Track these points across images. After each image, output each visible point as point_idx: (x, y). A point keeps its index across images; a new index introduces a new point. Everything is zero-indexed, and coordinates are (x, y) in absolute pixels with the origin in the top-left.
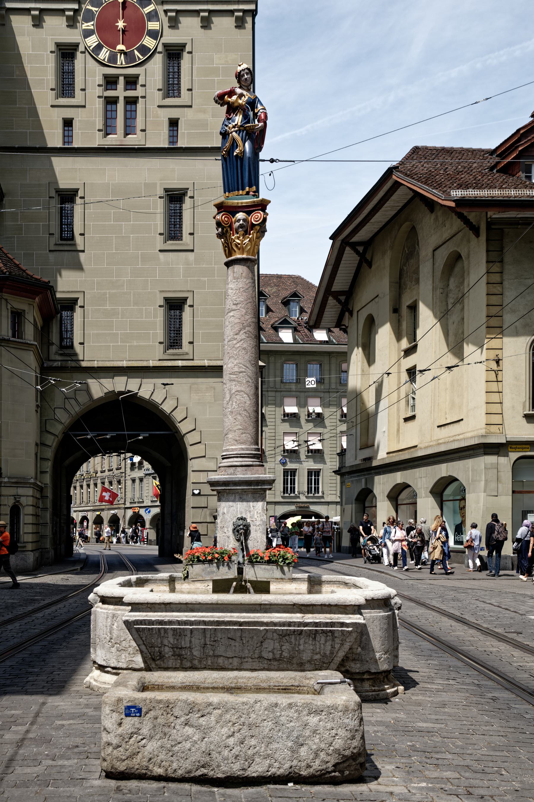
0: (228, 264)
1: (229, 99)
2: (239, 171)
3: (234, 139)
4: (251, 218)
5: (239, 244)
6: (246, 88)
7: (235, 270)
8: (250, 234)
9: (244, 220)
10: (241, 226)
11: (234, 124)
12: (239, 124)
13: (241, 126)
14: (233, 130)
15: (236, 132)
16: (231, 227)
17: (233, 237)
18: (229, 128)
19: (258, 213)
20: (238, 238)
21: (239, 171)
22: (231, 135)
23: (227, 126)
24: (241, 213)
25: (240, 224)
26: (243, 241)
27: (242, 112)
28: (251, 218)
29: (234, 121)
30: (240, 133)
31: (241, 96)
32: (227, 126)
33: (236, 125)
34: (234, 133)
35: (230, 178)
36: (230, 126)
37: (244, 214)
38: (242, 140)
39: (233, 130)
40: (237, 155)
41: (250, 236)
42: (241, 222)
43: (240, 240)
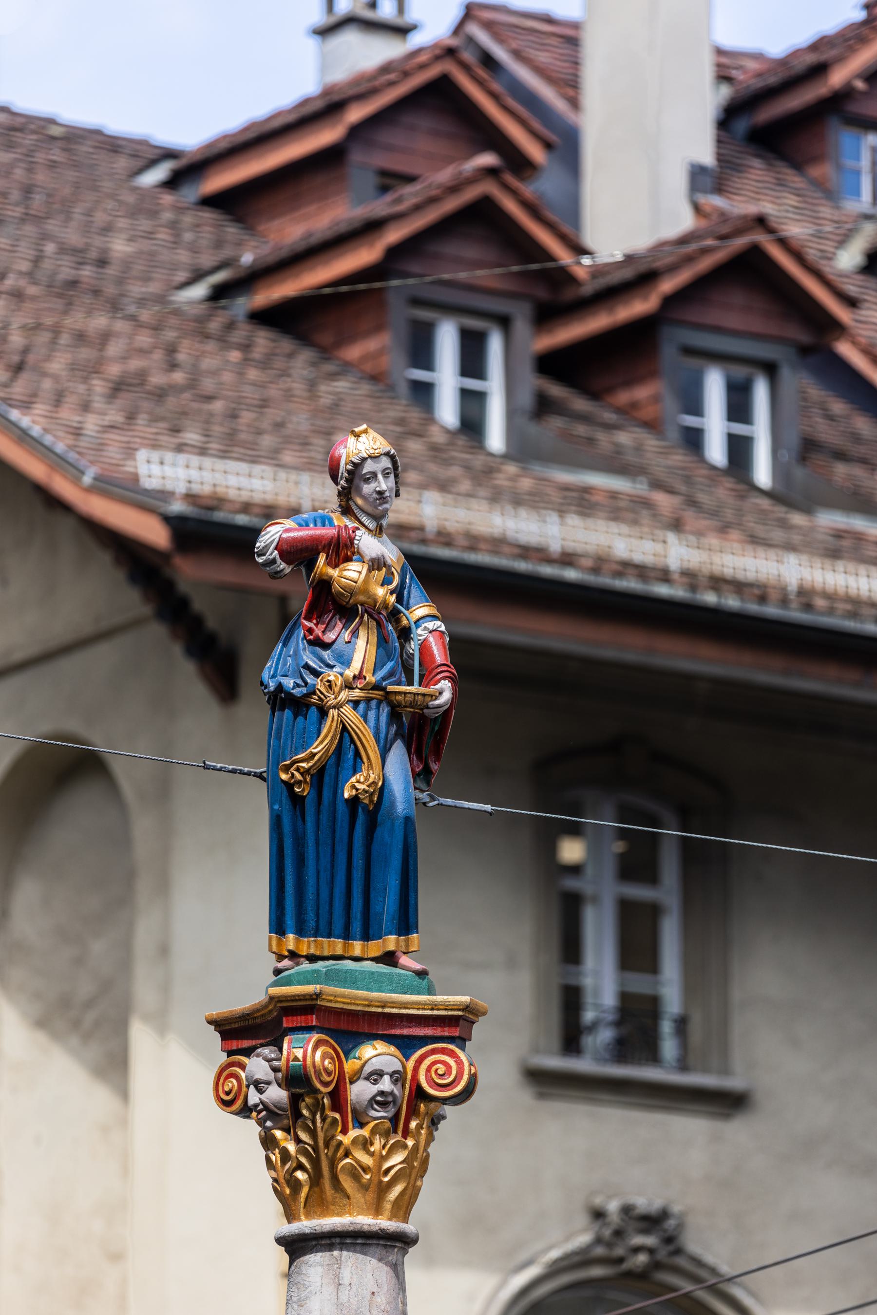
0: (296, 1246)
1: (334, 573)
2: (358, 862)
3: (344, 729)
4: (416, 1069)
5: (366, 1169)
6: (372, 525)
7: (346, 1275)
8: (406, 1133)
9: (398, 1077)
10: (382, 1100)
11: (350, 673)
12: (371, 678)
13: (376, 687)
14: (344, 695)
15: (356, 704)
16: (338, 1098)
17: (346, 1140)
18: (330, 685)
19: (443, 1051)
20: (365, 1144)
21: (358, 862)
22: (333, 713)
23: (316, 674)
24: (381, 1047)
25: (382, 1093)
26: (384, 1158)
27: (373, 624)
28: (416, 1069)
29: (347, 663)
30: (368, 708)
31: (377, 564)
32: (316, 674)
33: (355, 677)
34: (347, 710)
35: (311, 881)
36: (332, 675)
37: (392, 1049)
38: (378, 741)
39: (344, 695)
40: (354, 801)
41: (410, 1143)
42: (386, 1085)
43: (372, 1154)
